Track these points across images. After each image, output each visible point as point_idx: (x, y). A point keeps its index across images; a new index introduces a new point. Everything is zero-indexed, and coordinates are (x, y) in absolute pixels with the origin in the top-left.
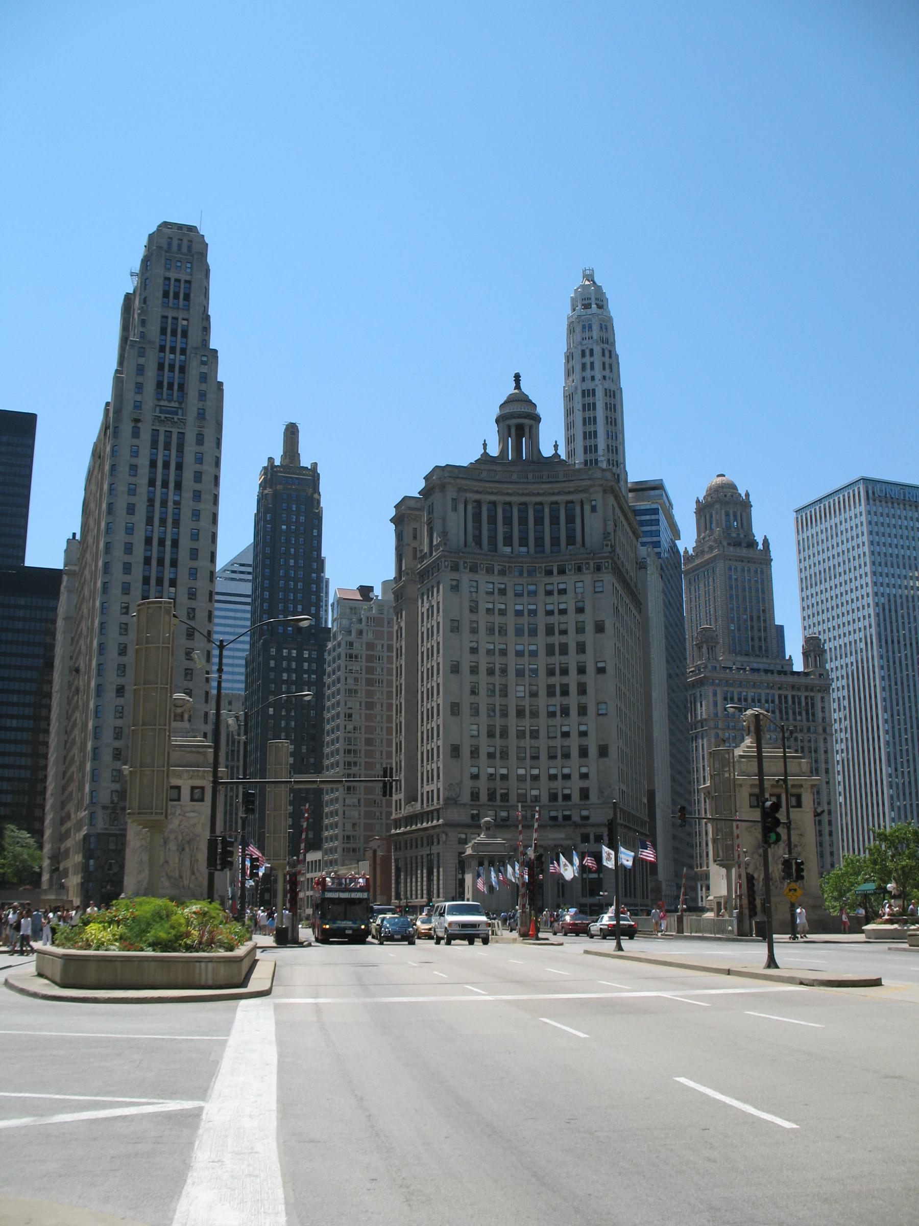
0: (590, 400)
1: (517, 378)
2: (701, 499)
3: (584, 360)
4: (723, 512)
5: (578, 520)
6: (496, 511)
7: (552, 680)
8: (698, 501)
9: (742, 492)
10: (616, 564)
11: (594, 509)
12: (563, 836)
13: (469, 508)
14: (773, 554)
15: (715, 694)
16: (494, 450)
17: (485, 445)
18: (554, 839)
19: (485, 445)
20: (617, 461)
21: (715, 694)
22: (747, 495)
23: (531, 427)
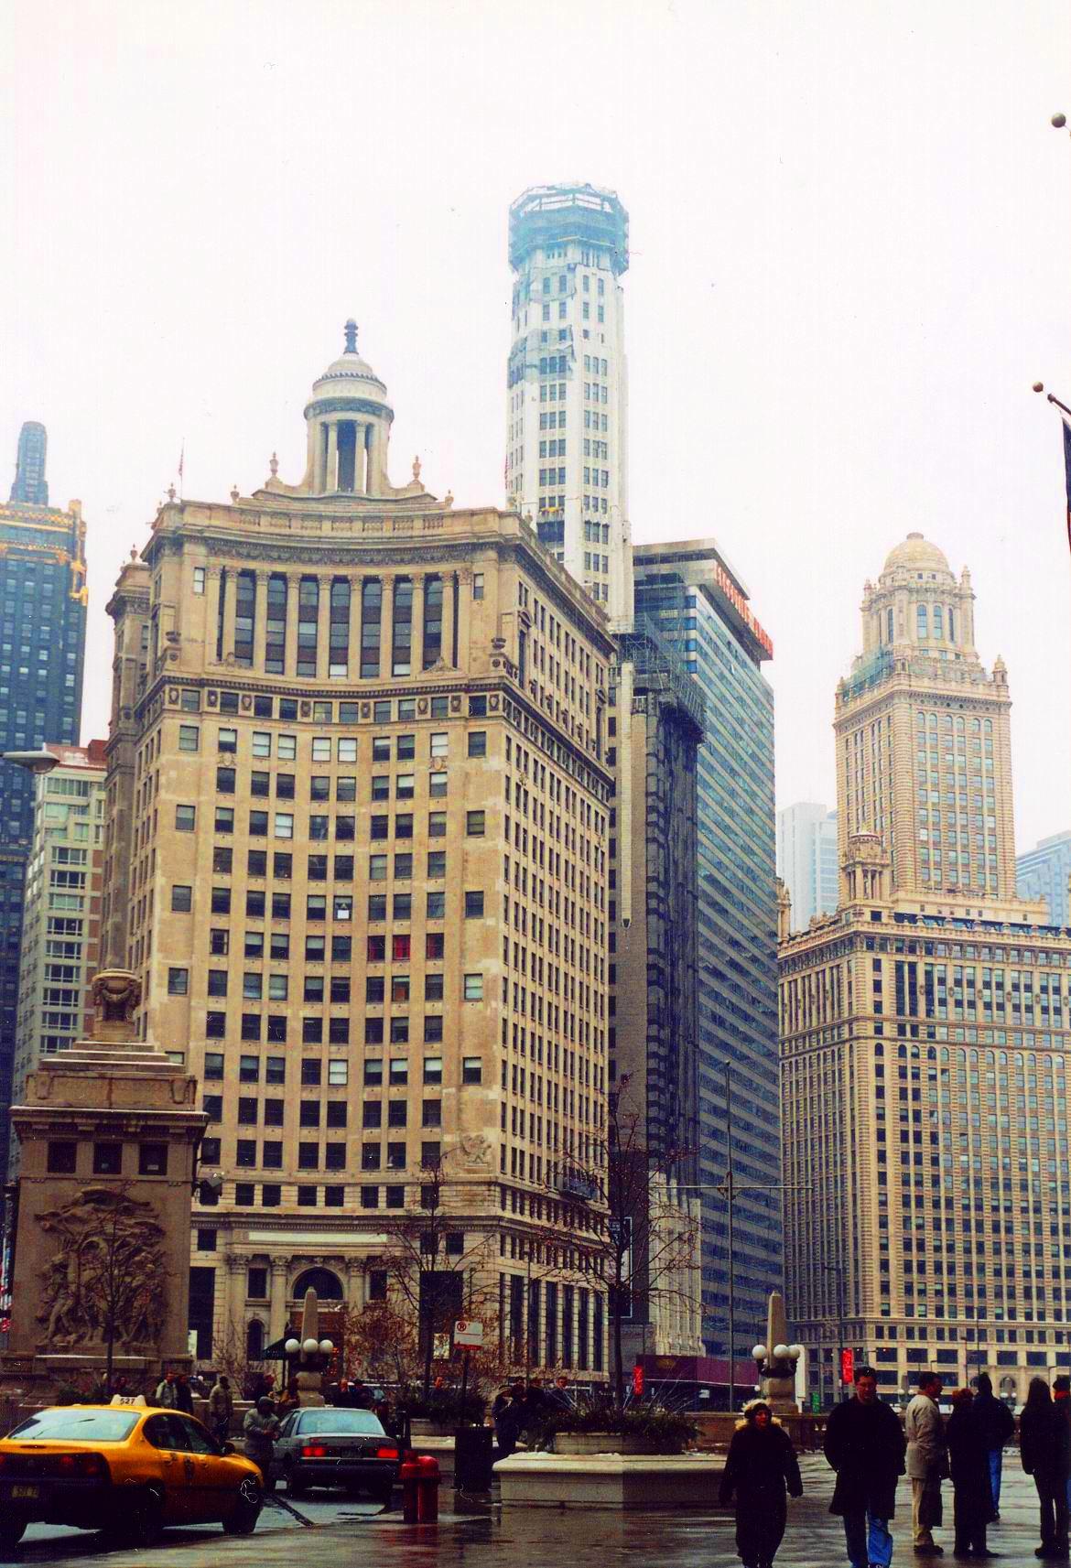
1: (351, 331)
2: (874, 582)
4: (914, 607)
5: (447, 613)
6: (254, 590)
7: (378, 929)
8: (868, 588)
9: (957, 570)
10: (518, 700)
11: (478, 593)
12: (383, 1238)
13: (231, 587)
14: (1015, 692)
15: (877, 965)
16: (294, 473)
17: (274, 462)
18: (367, 1245)
19: (274, 462)
21: (877, 965)
22: (966, 575)
23: (369, 428)
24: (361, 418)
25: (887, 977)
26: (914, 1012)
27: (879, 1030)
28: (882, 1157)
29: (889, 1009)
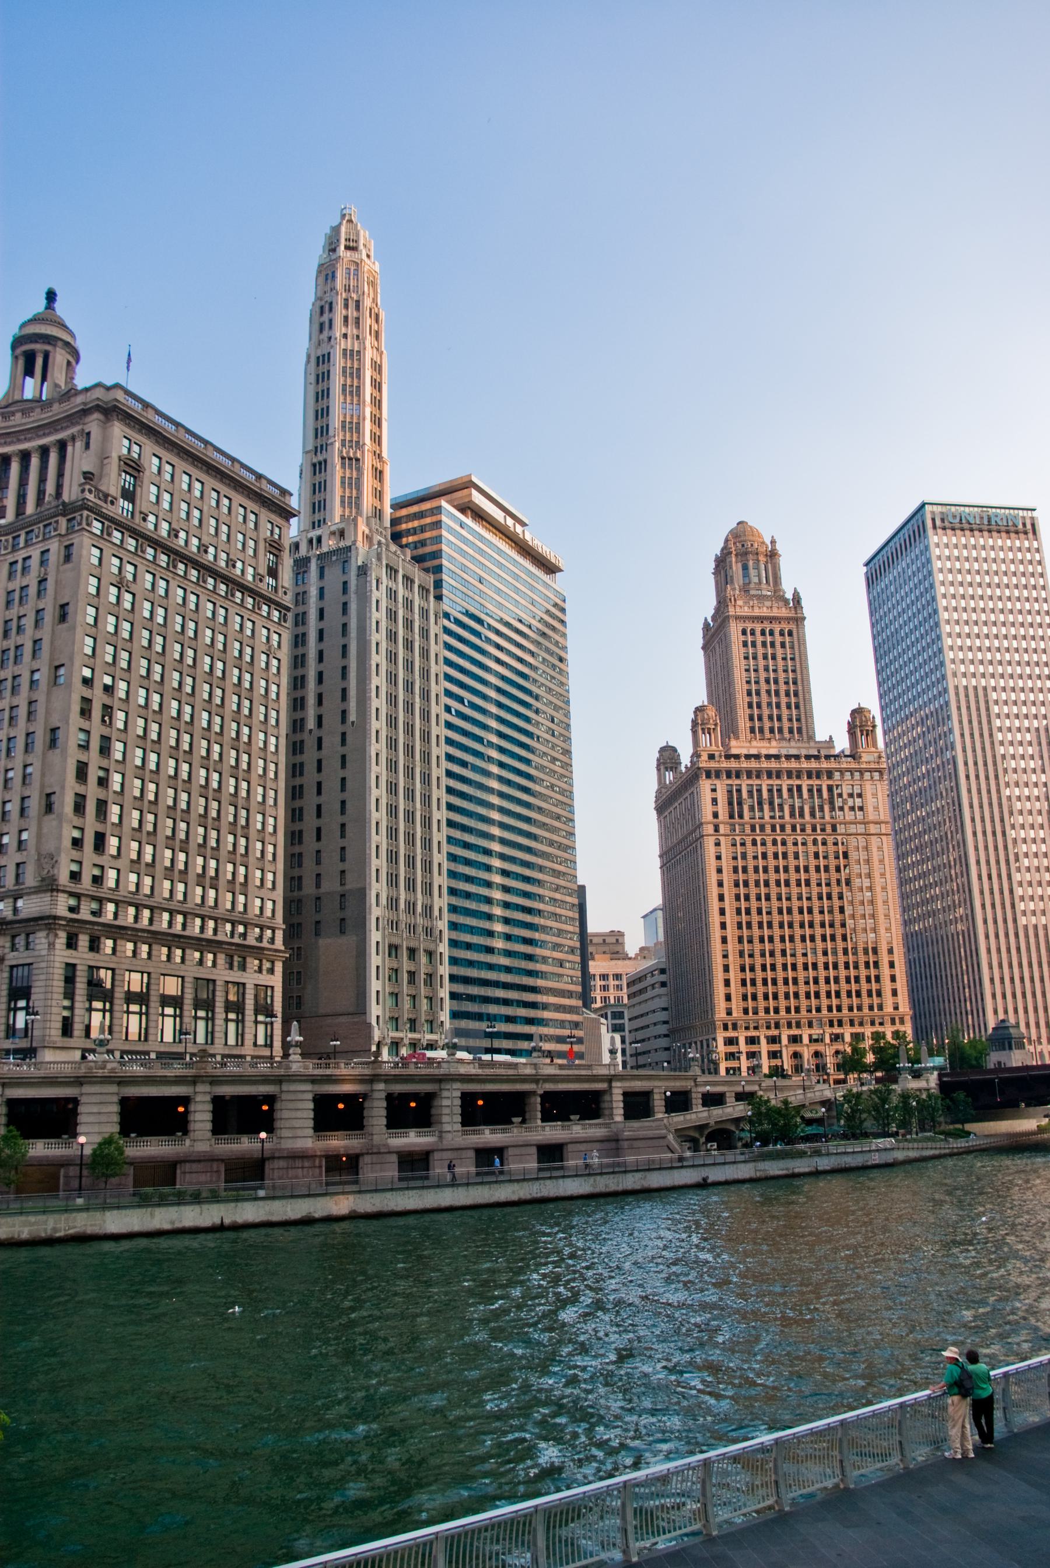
0: (323, 368)
1: (51, 296)
3: (322, 319)
4: (740, 565)
15: (714, 790)
20: (358, 442)
21: (714, 790)
22: (773, 542)
24: (37, 347)
25: (721, 796)
26: (741, 816)
27: (717, 830)
28: (722, 912)
29: (723, 815)
